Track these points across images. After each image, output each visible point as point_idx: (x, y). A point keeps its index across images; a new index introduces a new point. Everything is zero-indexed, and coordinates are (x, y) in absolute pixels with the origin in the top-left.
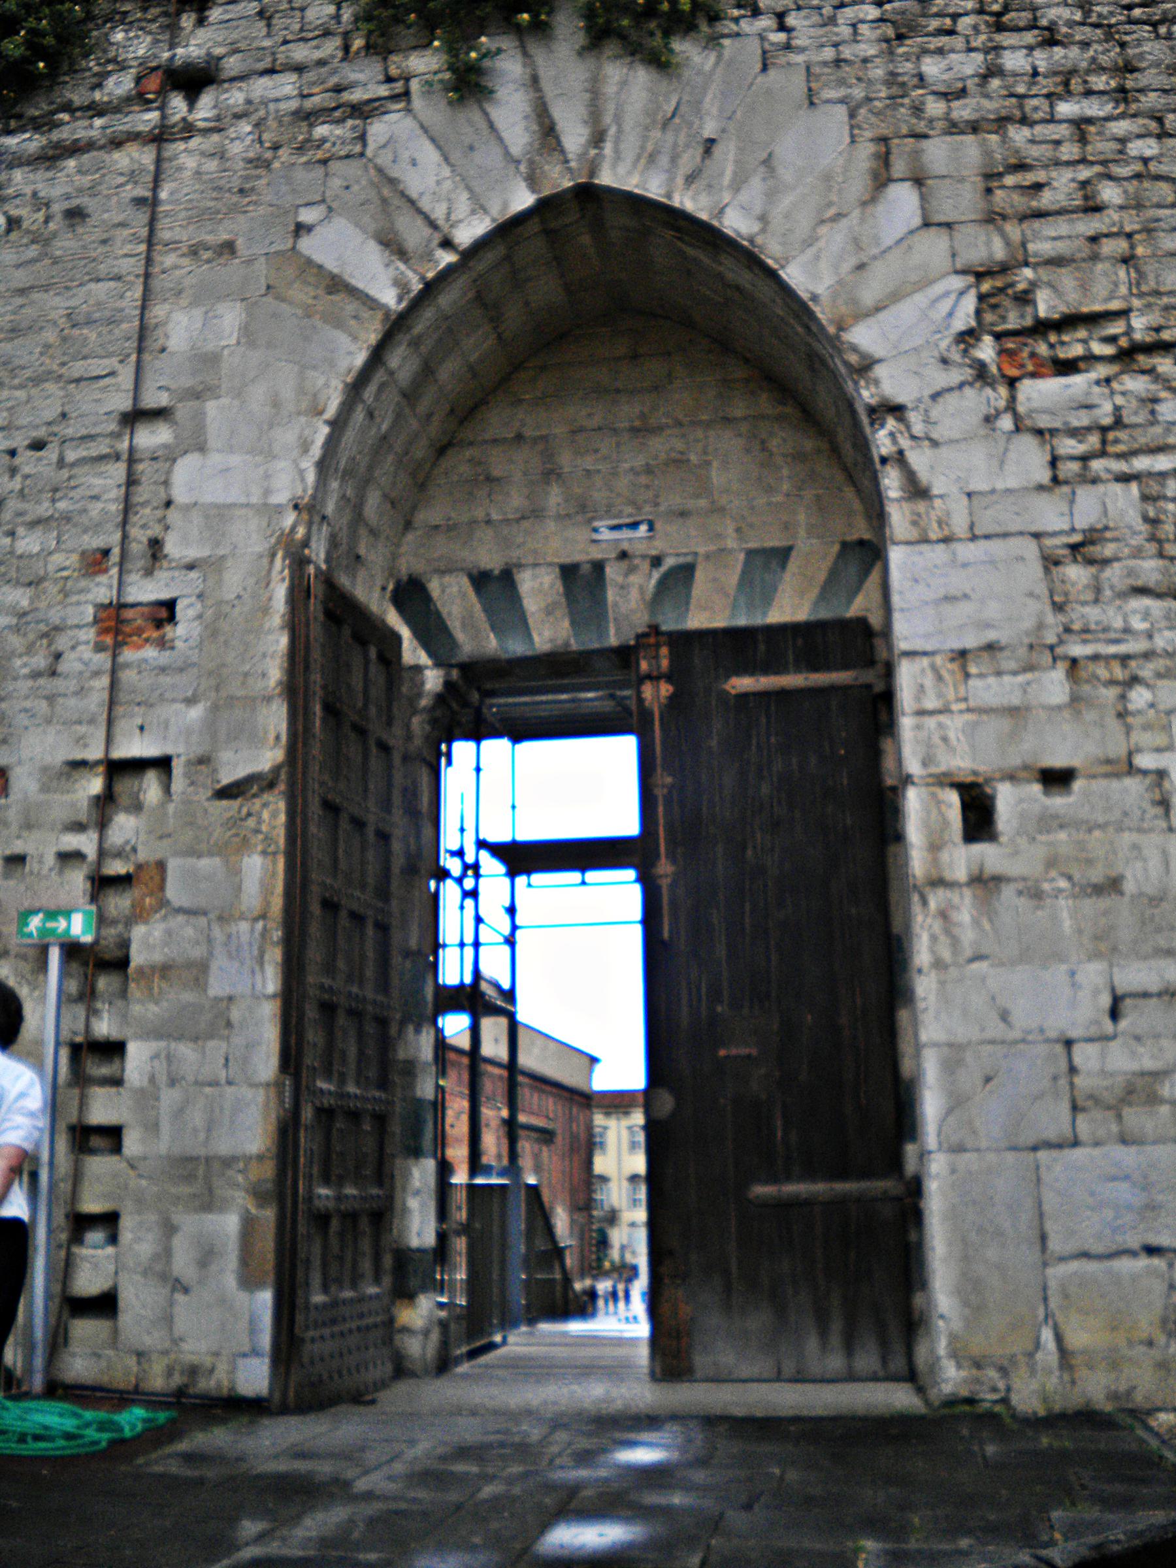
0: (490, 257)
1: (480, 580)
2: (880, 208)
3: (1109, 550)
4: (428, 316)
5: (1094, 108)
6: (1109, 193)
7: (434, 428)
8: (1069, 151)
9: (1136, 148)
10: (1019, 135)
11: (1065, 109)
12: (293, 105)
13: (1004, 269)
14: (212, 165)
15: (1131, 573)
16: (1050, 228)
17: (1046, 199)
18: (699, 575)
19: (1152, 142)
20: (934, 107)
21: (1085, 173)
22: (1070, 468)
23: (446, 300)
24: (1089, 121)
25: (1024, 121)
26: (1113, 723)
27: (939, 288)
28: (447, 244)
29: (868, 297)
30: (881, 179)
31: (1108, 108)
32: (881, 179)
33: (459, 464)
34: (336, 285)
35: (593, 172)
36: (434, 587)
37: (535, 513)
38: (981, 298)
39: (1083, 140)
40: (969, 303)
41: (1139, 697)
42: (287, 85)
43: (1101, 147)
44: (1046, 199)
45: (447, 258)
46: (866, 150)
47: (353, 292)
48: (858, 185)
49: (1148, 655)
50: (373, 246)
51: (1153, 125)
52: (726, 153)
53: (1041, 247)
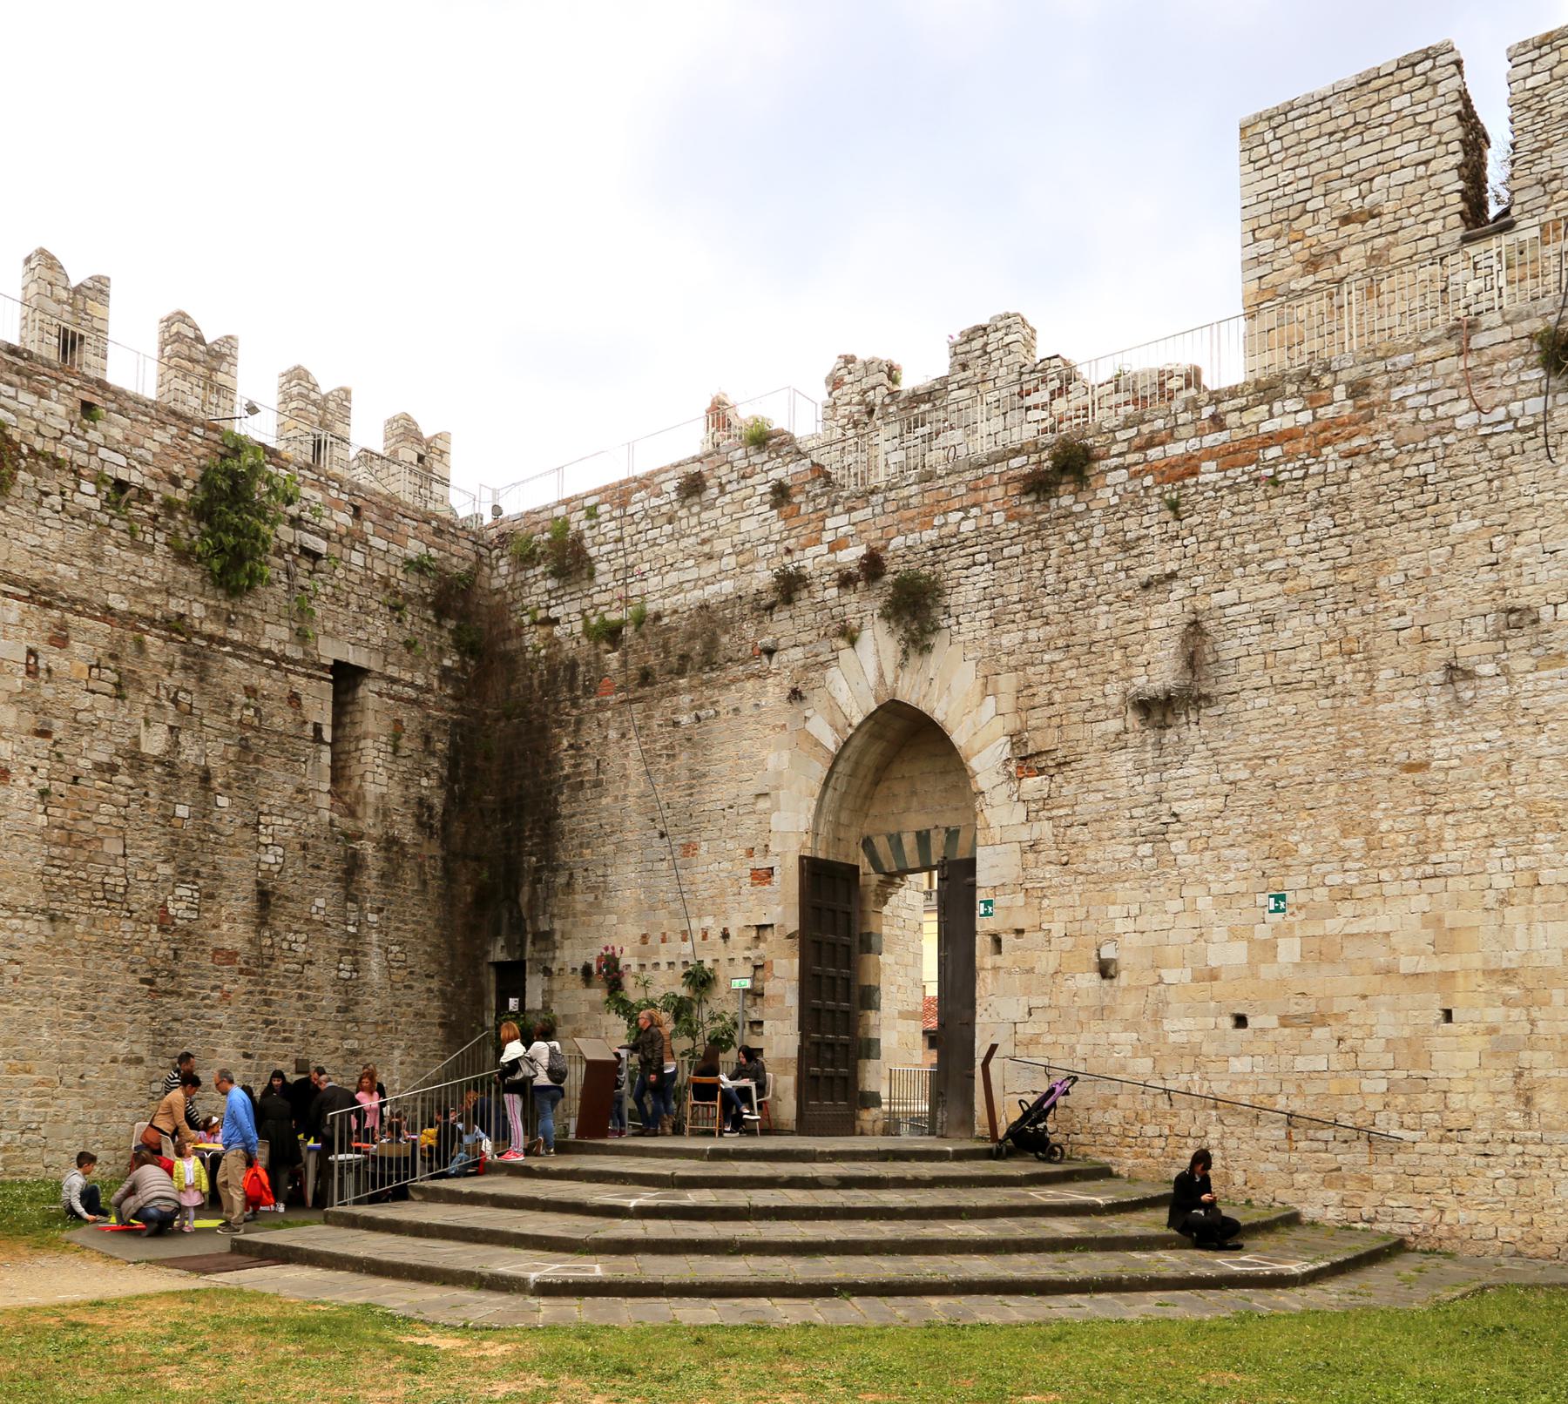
0: (864, 729)
1: (890, 837)
2: (982, 708)
3: (1041, 847)
4: (847, 754)
5: (1057, 656)
6: (1057, 697)
7: (870, 778)
8: (1046, 678)
9: (1071, 674)
10: (1030, 670)
11: (1047, 657)
12: (800, 663)
13: (1020, 733)
14: (777, 690)
15: (1047, 856)
16: (1038, 713)
17: (1037, 701)
18: (961, 834)
19: (1074, 671)
20: (1004, 659)
21: (1050, 687)
22: (1033, 815)
23: (856, 742)
24: (1054, 662)
25: (1033, 664)
26: (1037, 912)
27: (998, 742)
28: (850, 725)
29: (977, 746)
30: (984, 695)
31: (1062, 656)
32: (984, 695)
33: (883, 787)
34: (818, 744)
35: (894, 695)
36: (875, 841)
37: (907, 810)
38: (1013, 744)
39: (1051, 672)
40: (1008, 747)
41: (1045, 902)
42: (797, 653)
43: (1058, 674)
44: (1037, 701)
45: (850, 731)
46: (981, 680)
47: (822, 745)
48: (976, 698)
49: (1049, 887)
50: (828, 727)
51: (1076, 662)
52: (936, 683)
53: (1032, 723)
